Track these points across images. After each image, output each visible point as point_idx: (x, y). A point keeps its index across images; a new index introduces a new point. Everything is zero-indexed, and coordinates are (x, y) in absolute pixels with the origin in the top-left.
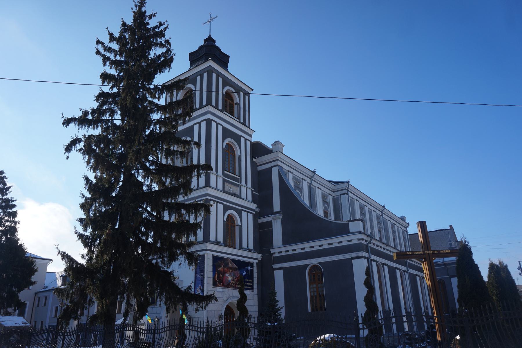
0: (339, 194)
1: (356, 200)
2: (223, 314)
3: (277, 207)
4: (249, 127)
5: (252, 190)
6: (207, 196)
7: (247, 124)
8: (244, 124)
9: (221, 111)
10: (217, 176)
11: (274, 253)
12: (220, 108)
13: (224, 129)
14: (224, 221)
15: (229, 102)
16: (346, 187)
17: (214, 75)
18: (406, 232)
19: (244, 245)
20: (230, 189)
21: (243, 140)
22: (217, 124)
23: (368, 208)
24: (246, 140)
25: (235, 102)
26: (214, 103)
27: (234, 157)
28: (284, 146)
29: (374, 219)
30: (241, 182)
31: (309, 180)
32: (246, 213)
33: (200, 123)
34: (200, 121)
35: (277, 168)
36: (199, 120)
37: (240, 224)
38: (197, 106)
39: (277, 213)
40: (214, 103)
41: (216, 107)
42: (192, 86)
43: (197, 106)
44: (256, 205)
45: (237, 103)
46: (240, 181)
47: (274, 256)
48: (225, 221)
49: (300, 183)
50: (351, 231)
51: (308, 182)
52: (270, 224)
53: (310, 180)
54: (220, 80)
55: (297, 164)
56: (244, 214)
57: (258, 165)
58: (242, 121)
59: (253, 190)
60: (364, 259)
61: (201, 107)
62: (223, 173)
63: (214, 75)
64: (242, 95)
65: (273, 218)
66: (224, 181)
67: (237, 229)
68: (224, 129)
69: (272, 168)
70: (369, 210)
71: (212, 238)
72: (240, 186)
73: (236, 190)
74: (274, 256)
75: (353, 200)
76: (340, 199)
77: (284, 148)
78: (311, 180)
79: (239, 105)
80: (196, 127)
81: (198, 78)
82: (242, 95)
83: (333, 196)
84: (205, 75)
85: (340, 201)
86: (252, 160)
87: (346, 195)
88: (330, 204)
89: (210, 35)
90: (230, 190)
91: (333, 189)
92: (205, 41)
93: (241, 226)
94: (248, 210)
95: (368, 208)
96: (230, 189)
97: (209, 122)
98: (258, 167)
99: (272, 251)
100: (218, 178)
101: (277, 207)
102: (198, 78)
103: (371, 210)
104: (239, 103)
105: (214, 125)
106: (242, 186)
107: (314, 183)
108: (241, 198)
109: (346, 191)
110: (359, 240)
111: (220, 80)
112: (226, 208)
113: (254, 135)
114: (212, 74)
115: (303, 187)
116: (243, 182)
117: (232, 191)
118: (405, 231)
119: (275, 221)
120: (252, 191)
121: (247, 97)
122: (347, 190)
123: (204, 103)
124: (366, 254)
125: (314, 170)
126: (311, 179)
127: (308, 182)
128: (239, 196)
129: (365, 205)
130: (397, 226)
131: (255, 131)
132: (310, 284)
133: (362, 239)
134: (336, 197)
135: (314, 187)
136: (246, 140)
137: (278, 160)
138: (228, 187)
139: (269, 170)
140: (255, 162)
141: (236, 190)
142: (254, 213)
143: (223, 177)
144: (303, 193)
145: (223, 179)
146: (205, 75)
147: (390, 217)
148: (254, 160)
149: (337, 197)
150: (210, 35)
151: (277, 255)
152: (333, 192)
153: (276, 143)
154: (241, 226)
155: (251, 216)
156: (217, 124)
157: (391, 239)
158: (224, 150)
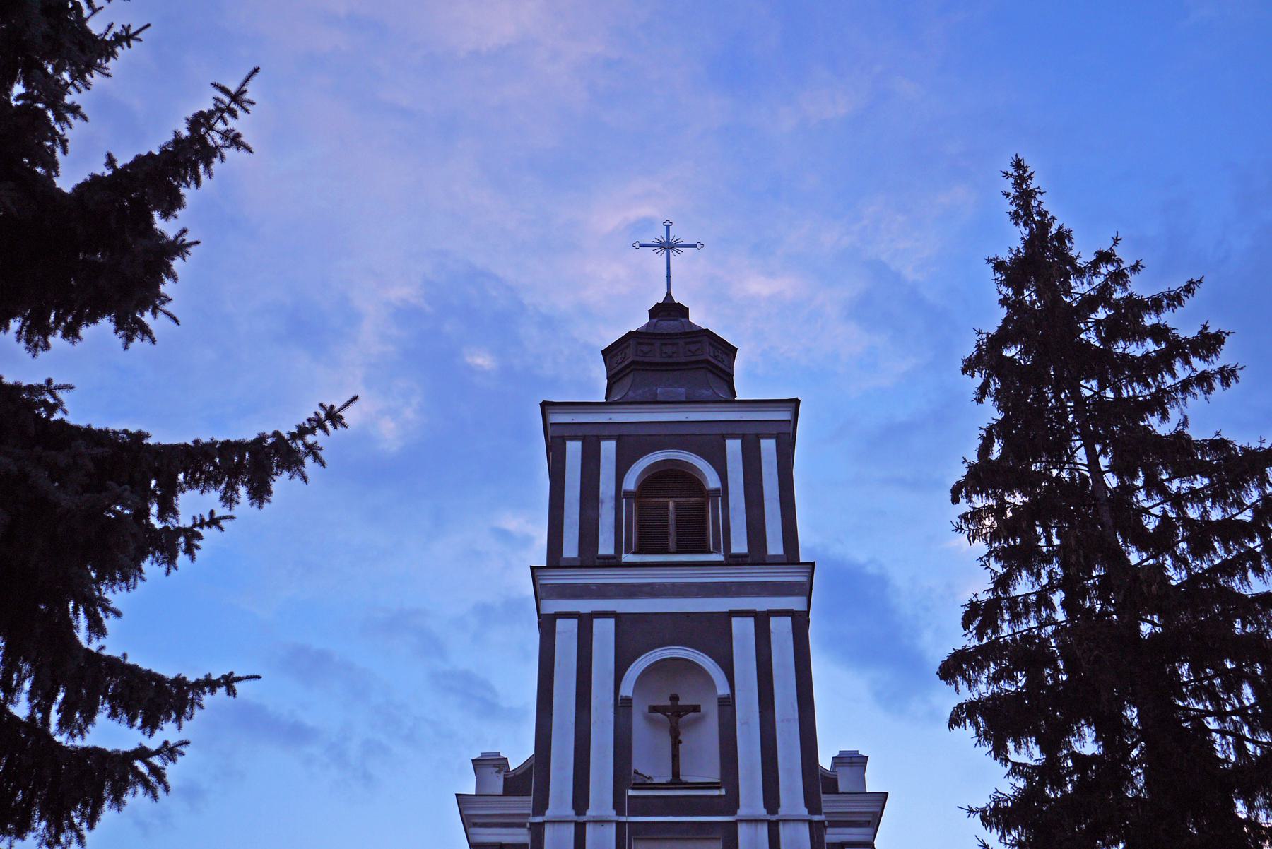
9: (611, 562)
10: (580, 829)
15: (677, 505)
26: (570, 549)
41: (589, 558)
46: (731, 803)
54: (608, 449)
62: (618, 806)
64: (734, 447)
72: (735, 823)
82: (734, 447)
89: (669, 294)
100: (589, 829)
105: (567, 631)
111: (608, 449)
150: (669, 294)
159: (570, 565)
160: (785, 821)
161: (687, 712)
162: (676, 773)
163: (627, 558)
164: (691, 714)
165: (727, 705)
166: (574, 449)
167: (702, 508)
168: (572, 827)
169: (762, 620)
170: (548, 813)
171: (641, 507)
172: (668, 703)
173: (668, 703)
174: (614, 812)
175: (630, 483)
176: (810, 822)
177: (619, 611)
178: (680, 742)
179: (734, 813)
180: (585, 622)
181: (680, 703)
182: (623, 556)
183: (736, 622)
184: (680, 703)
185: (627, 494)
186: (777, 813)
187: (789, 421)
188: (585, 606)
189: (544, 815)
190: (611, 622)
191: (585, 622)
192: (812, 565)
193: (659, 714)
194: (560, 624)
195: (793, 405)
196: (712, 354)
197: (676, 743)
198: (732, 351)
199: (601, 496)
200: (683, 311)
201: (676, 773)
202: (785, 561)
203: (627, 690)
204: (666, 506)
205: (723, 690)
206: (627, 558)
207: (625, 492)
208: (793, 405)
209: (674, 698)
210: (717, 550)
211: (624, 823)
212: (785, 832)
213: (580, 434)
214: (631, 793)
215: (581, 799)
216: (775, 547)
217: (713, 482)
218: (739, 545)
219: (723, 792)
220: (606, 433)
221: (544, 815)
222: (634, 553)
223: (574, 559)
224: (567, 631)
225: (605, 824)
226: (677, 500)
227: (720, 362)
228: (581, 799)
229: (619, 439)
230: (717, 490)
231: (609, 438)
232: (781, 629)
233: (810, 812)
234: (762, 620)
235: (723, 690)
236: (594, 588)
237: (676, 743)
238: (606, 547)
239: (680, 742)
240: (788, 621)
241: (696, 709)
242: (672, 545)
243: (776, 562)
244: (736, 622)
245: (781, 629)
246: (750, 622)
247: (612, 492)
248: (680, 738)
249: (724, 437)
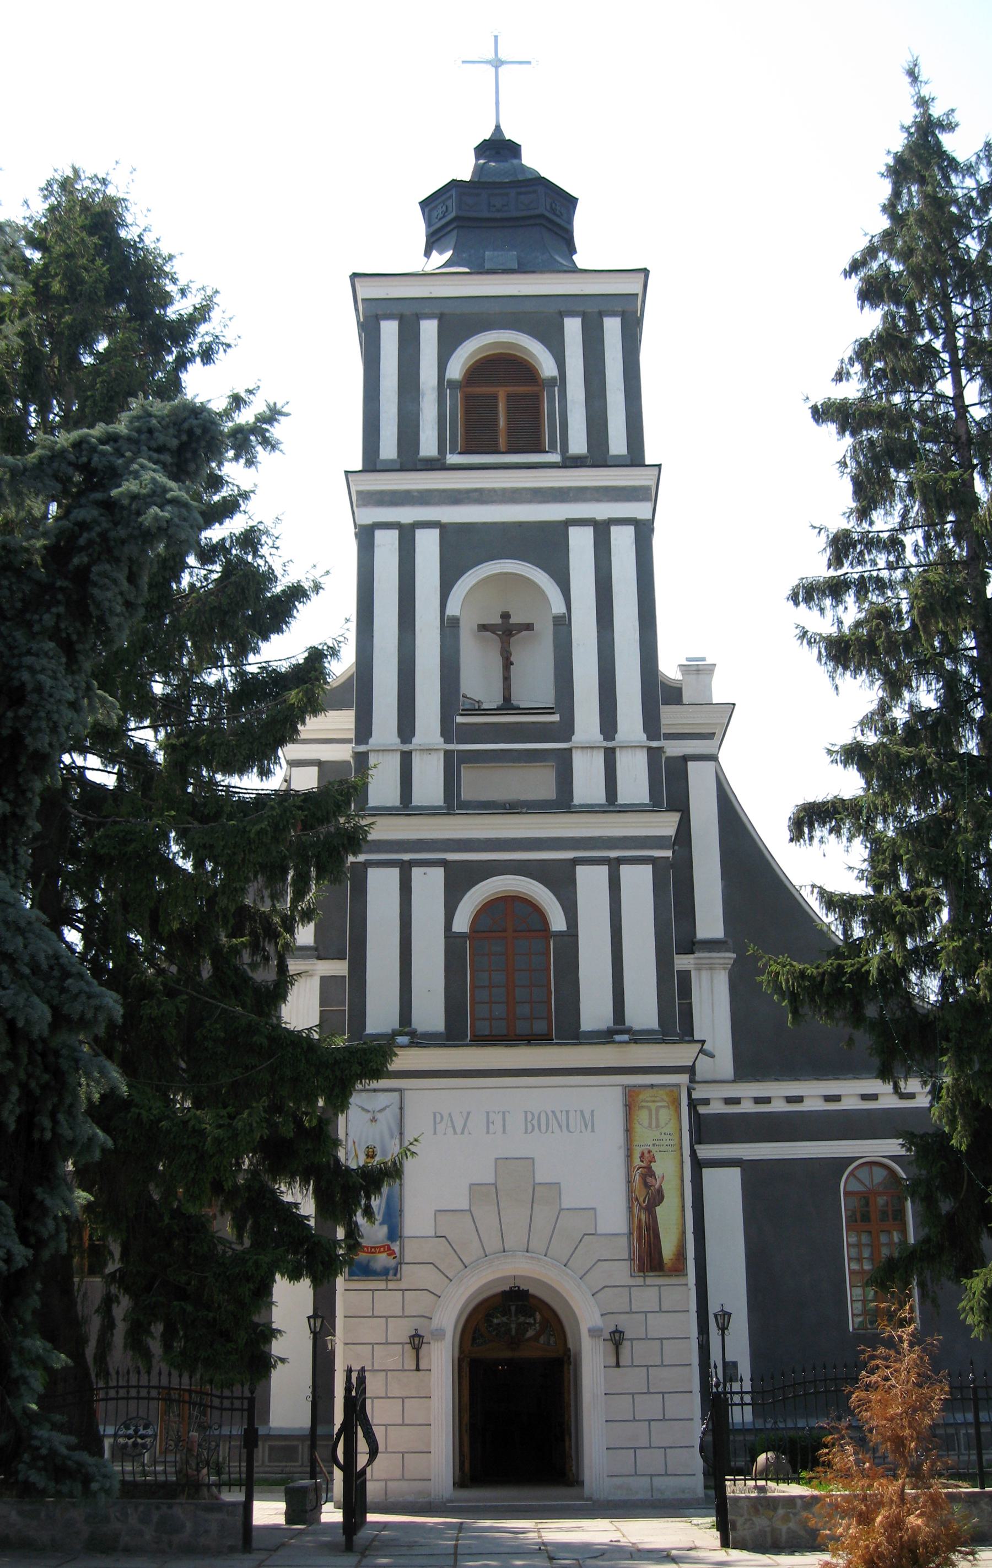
4: (635, 457)
14: (450, 935)
15: (510, 397)
26: (389, 449)
46: (566, 729)
48: (461, 936)
54: (429, 330)
62: (446, 733)
64: (573, 327)
66: (452, 764)
72: (570, 750)
82: (573, 327)
89: (498, 128)
94: (614, 854)
100: (417, 760)
111: (429, 330)
121: (612, 327)
145: (448, 755)
150: (498, 128)
159: (388, 468)
160: (621, 747)
161: (520, 631)
162: (507, 699)
163: (452, 459)
164: (524, 633)
165: (563, 624)
166: (389, 330)
167: (537, 398)
168: (397, 758)
169: (602, 530)
170: (371, 741)
171: (468, 398)
172: (499, 621)
173: (499, 621)
174: (442, 740)
175: (455, 370)
176: (650, 749)
177: (445, 520)
178: (512, 664)
179: (569, 740)
180: (407, 534)
181: (512, 621)
182: (448, 456)
183: (573, 531)
184: (512, 621)
185: (451, 383)
186: (614, 739)
187: (637, 295)
188: (407, 515)
189: (367, 743)
190: (435, 533)
191: (407, 534)
192: (659, 466)
193: (488, 633)
194: (379, 534)
195: (642, 275)
196: (548, 207)
197: (507, 664)
198: (571, 202)
199: (422, 387)
200: (513, 149)
201: (507, 699)
202: (629, 463)
203: (453, 609)
204: (495, 397)
205: (558, 607)
206: (452, 459)
207: (450, 382)
208: (642, 275)
209: (505, 616)
210: (553, 449)
211: (453, 751)
212: (623, 760)
213: (395, 312)
214: (459, 719)
215: (406, 727)
216: (618, 444)
217: (548, 367)
218: (578, 444)
219: (556, 718)
220: (427, 311)
221: (367, 743)
222: (460, 453)
223: (392, 461)
224: (387, 543)
225: (433, 753)
227: (558, 216)
228: (406, 727)
229: (441, 318)
230: (554, 379)
231: (429, 316)
232: (623, 539)
233: (649, 738)
234: (602, 530)
235: (558, 607)
236: (416, 494)
237: (507, 664)
238: (428, 446)
239: (512, 664)
240: (630, 530)
241: (529, 627)
242: (502, 442)
243: (619, 463)
244: (573, 531)
245: (623, 539)
246: (589, 532)
247: (434, 382)
248: (512, 659)
249: (562, 315)
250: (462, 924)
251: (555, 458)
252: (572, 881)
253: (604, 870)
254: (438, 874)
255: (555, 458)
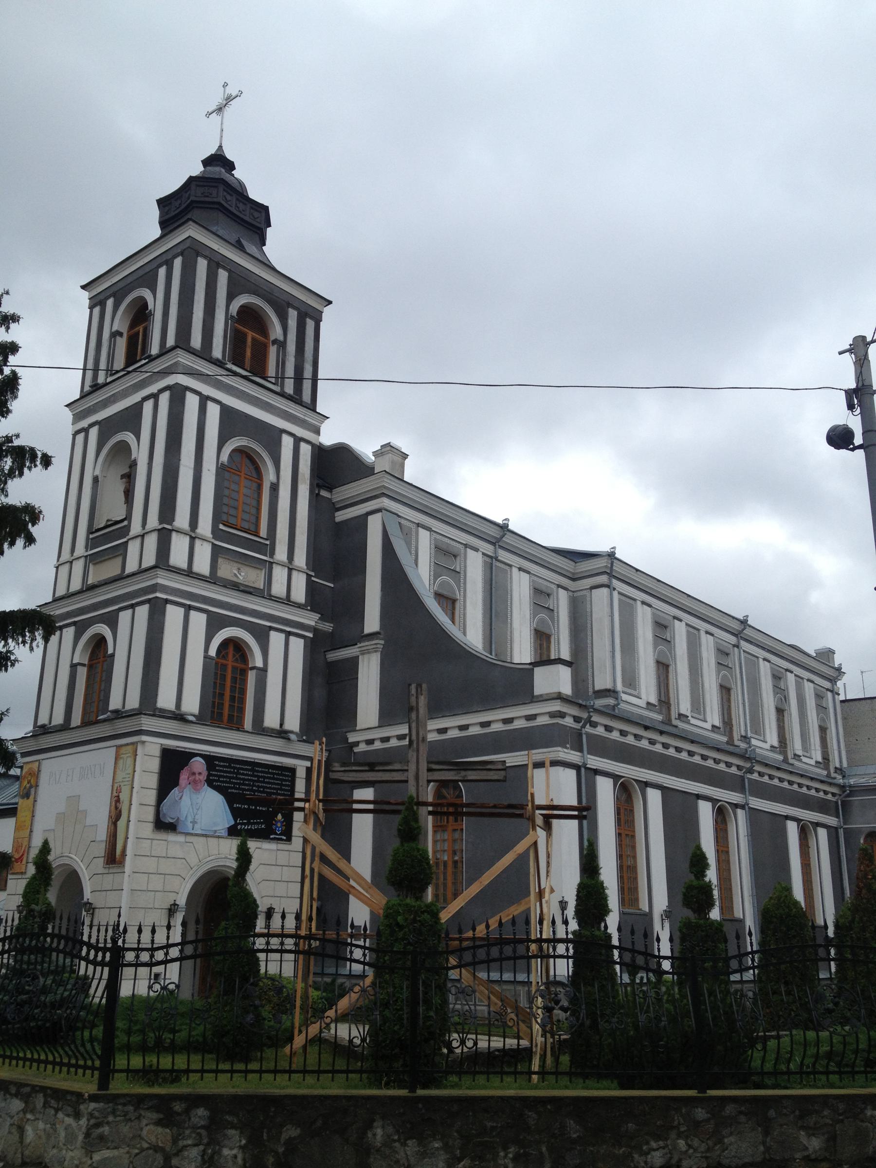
0: (589, 587)
1: (643, 603)
2: (182, 901)
3: (372, 622)
4: (312, 407)
5: (307, 574)
6: (155, 592)
7: (306, 397)
8: (296, 398)
11: (357, 744)
12: (217, 352)
13: (227, 412)
14: (206, 657)
15: (253, 339)
16: (606, 566)
17: (202, 265)
18: (829, 694)
19: (271, 720)
20: (236, 572)
21: (287, 443)
22: (204, 400)
23: (687, 625)
24: (298, 440)
25: (272, 338)
26: (196, 341)
27: (260, 487)
28: (406, 458)
29: (705, 654)
30: (272, 554)
31: (488, 549)
32: (283, 636)
33: (155, 396)
34: (155, 391)
35: (379, 516)
36: (153, 389)
37: (259, 663)
38: (155, 350)
39: (372, 636)
40: (196, 341)
41: (204, 354)
42: (146, 294)
43: (155, 350)
44: (317, 616)
45: (275, 342)
47: (356, 750)
48: (211, 658)
49: (458, 558)
50: (537, 692)
51: (484, 554)
52: (352, 665)
53: (491, 547)
54: (223, 276)
55: (447, 504)
56: (276, 640)
57: (337, 506)
58: (289, 388)
59: (313, 574)
60: (562, 768)
61: (164, 352)
62: (215, 531)
63: (202, 265)
64: (293, 315)
65: (360, 649)
66: (217, 552)
67: (252, 676)
68: (227, 412)
69: (370, 518)
70: (691, 630)
71: (166, 699)
72: (271, 563)
73: (253, 577)
74: (356, 750)
75: (631, 602)
76: (588, 599)
77: (407, 461)
78: (495, 548)
79: (282, 345)
80: (148, 406)
81: (162, 271)
82: (293, 315)
83: (573, 592)
84: (178, 263)
85: (588, 606)
86: (314, 497)
87: (605, 590)
88: (558, 613)
89: (220, 147)
90: (235, 575)
91: (573, 574)
92: (207, 162)
93: (263, 671)
95: (687, 625)
96: (236, 572)
97: (178, 394)
98: (337, 514)
99: (352, 738)
101: (372, 622)
102: (162, 271)
103: (698, 630)
104: (281, 338)
105: (192, 402)
106: (274, 565)
107: (503, 555)
108: (271, 598)
109: (604, 579)
110: (552, 715)
111: (223, 276)
112: (215, 624)
113: (325, 428)
114: (196, 262)
115: (465, 567)
116: (281, 554)
117: (241, 578)
118: (827, 690)
119: (366, 656)
120: (309, 576)
121: (310, 324)
122: (611, 574)
123: (171, 342)
124: (574, 757)
125: (505, 522)
126: (494, 544)
127: (484, 554)
128: (265, 594)
129: (675, 618)
130: (796, 675)
131: (328, 418)
132: (435, 832)
133: (562, 715)
134: (579, 594)
135: (507, 568)
136: (298, 440)
137: (384, 495)
138: (227, 570)
139: (361, 522)
140: (330, 500)
141: (253, 577)
142: (310, 635)
143: (213, 541)
144: (465, 583)
145: (213, 544)
146: (178, 263)
147: (769, 651)
148: (324, 493)
149: (582, 593)
150: (220, 147)
151: (362, 747)
152: (574, 580)
153: (388, 449)
154: (264, 670)
155: (297, 646)
156: (204, 400)
157: (766, 712)
158: (221, 469)
163: (229, 366)
174: (211, 536)
185: (232, 317)
200: (230, 166)
206: (229, 366)
217: (276, 331)
219: (268, 542)
226: (254, 334)
229: (230, 271)
250: (213, 652)
251: (277, 388)
252: (268, 637)
253: (283, 636)
254: (203, 617)
255: (277, 388)
